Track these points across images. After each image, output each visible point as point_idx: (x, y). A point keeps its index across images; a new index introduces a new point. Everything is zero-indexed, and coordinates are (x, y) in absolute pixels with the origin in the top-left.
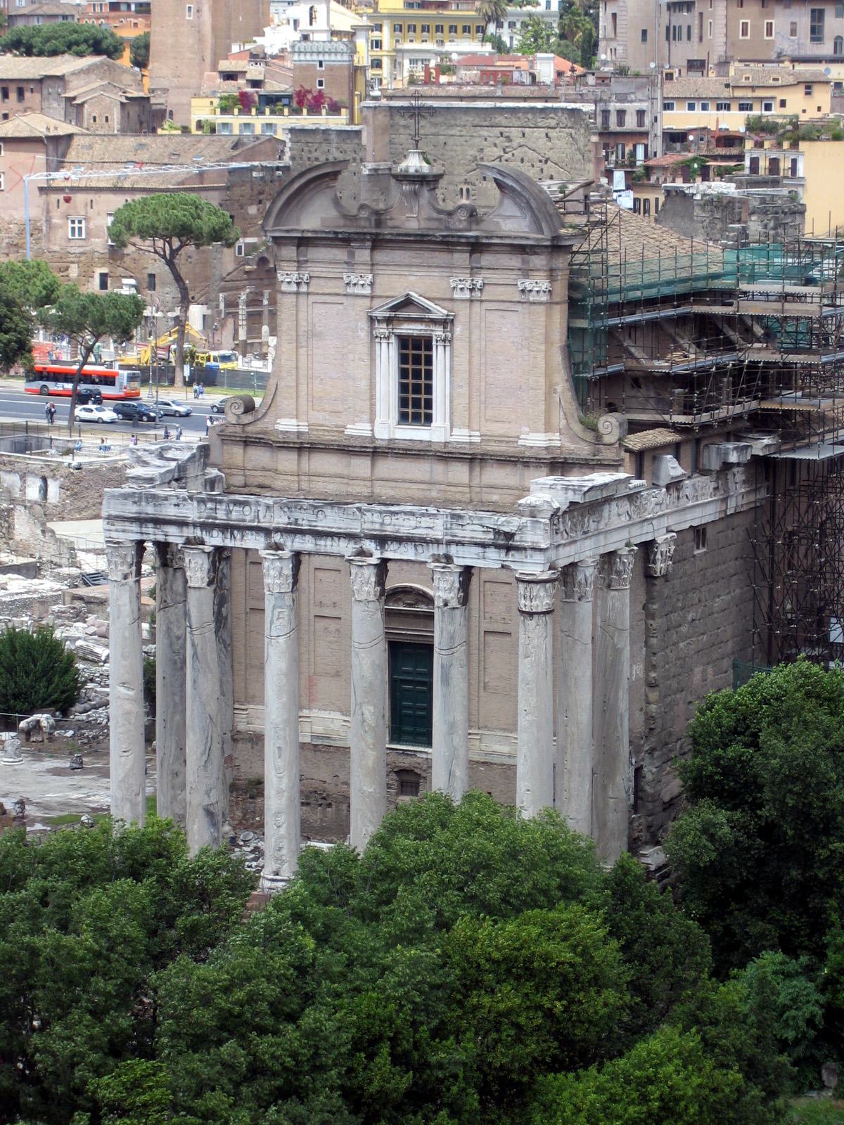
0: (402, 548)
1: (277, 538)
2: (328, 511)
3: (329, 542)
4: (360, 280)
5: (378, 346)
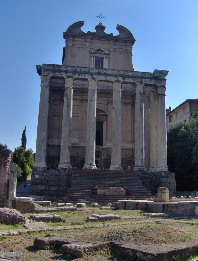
0: (129, 79)
1: (94, 76)
2: (109, 70)
3: (109, 77)
4: (88, 45)
5: (91, 58)
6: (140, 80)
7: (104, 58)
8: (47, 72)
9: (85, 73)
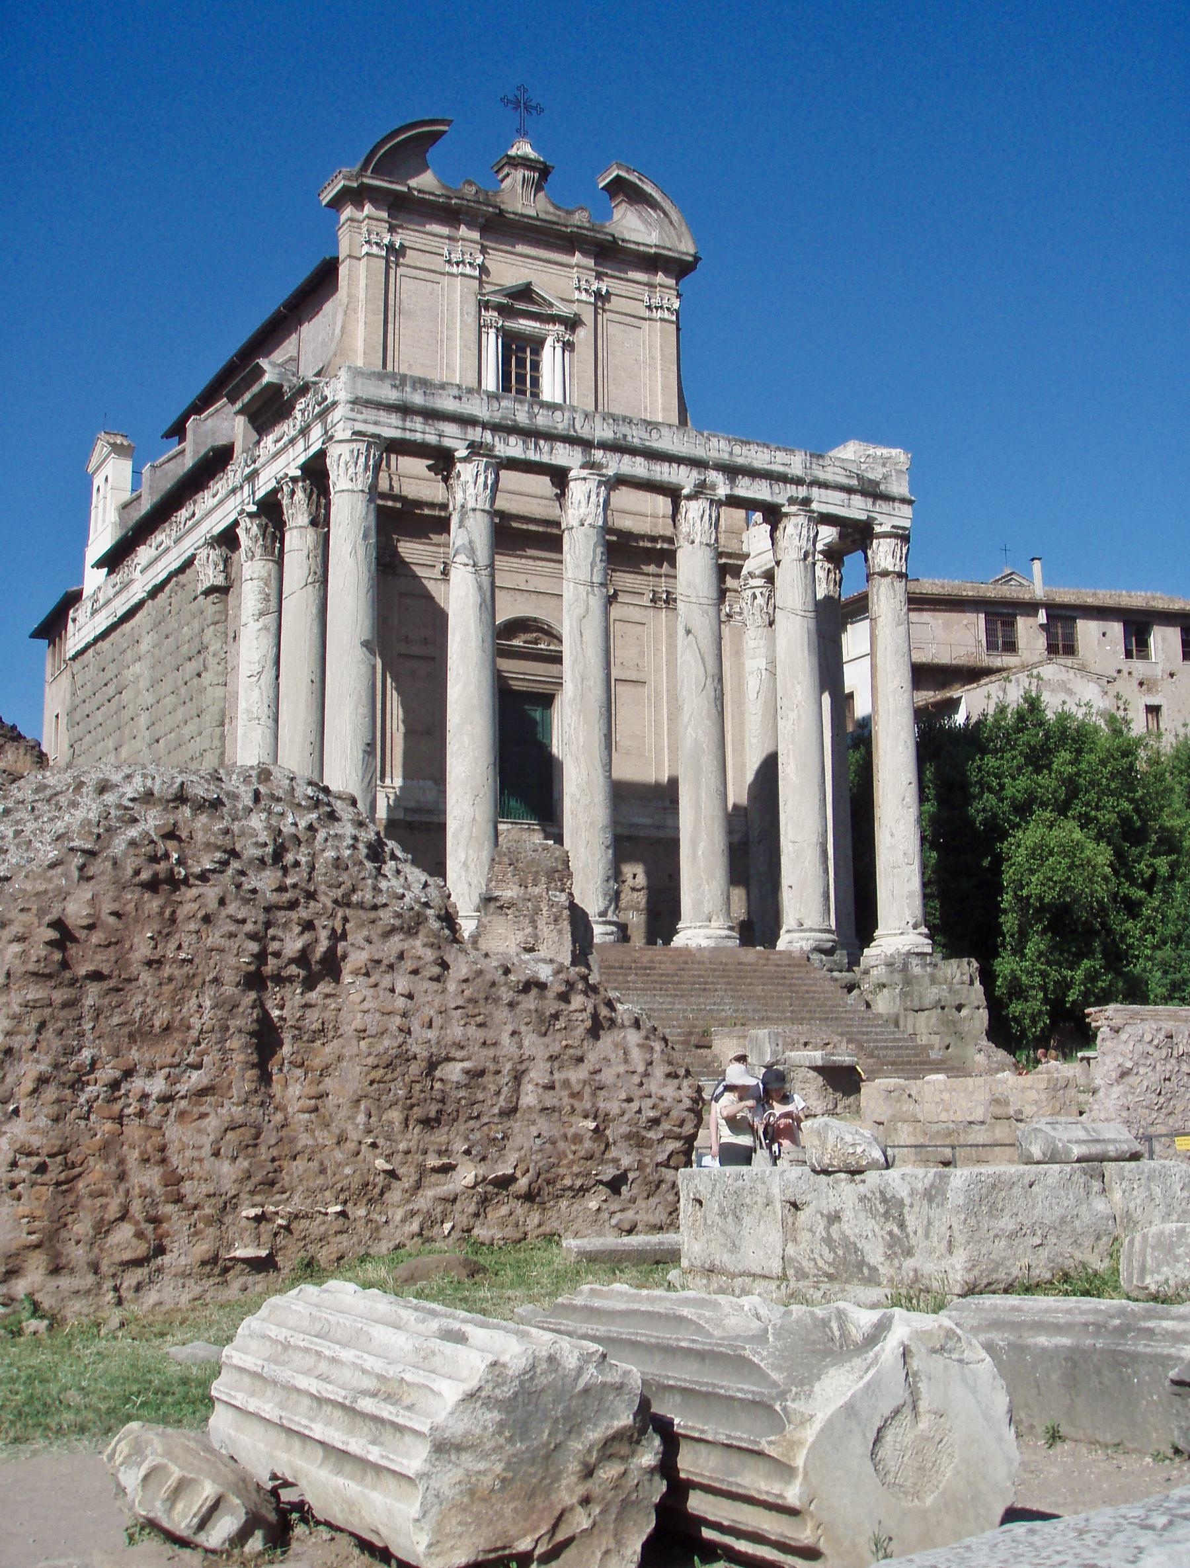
1: (598, 455)
5: (484, 336)
6: (802, 492)
7: (549, 342)
8: (370, 414)
9: (551, 437)
